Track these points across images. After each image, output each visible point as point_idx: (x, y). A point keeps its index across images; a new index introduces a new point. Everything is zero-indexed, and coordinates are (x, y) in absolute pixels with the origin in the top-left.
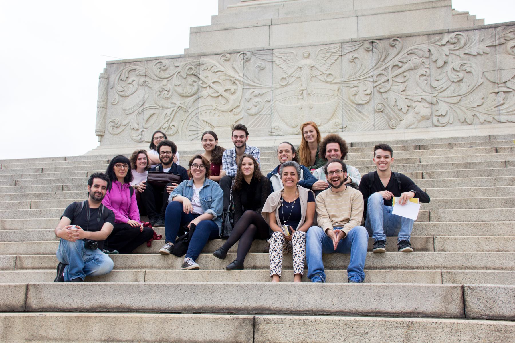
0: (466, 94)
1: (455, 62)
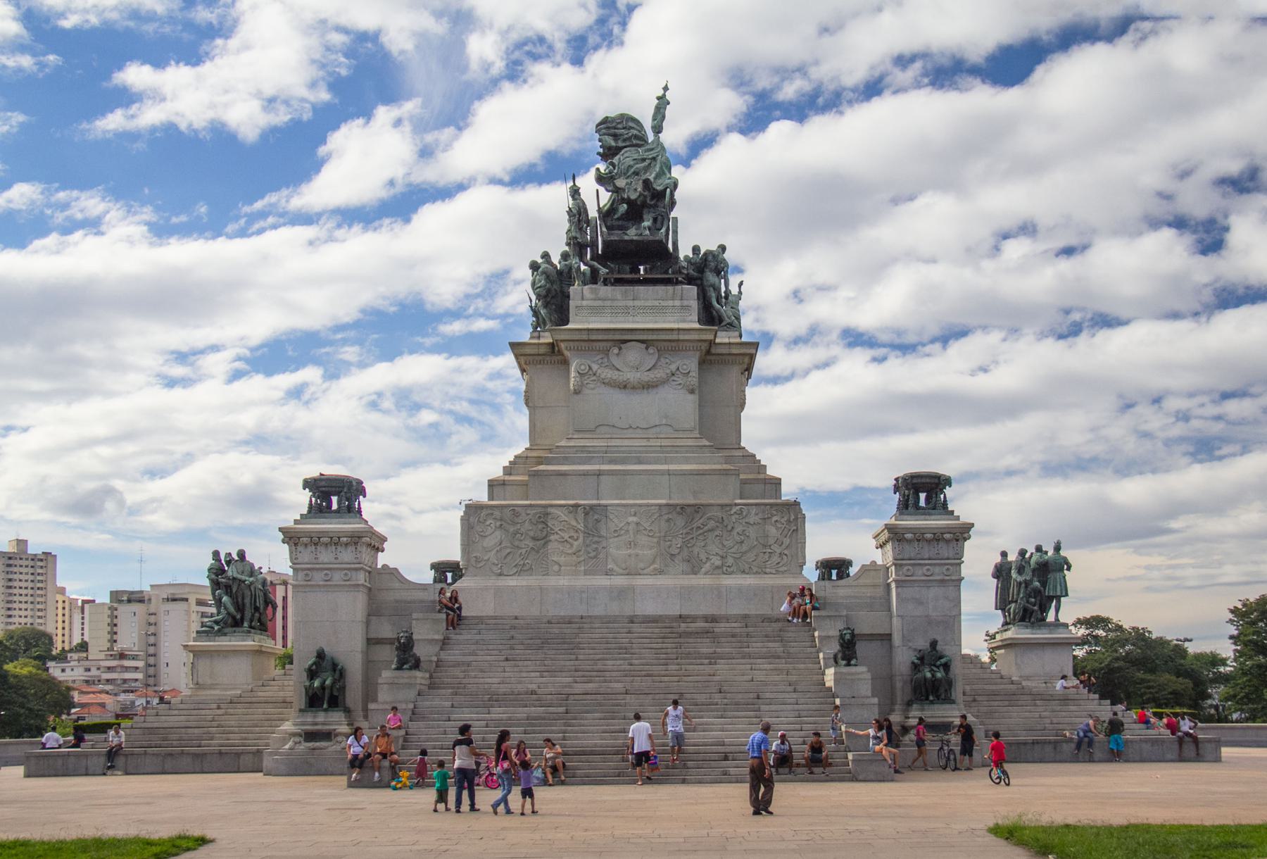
0: (745, 552)
1: (739, 529)
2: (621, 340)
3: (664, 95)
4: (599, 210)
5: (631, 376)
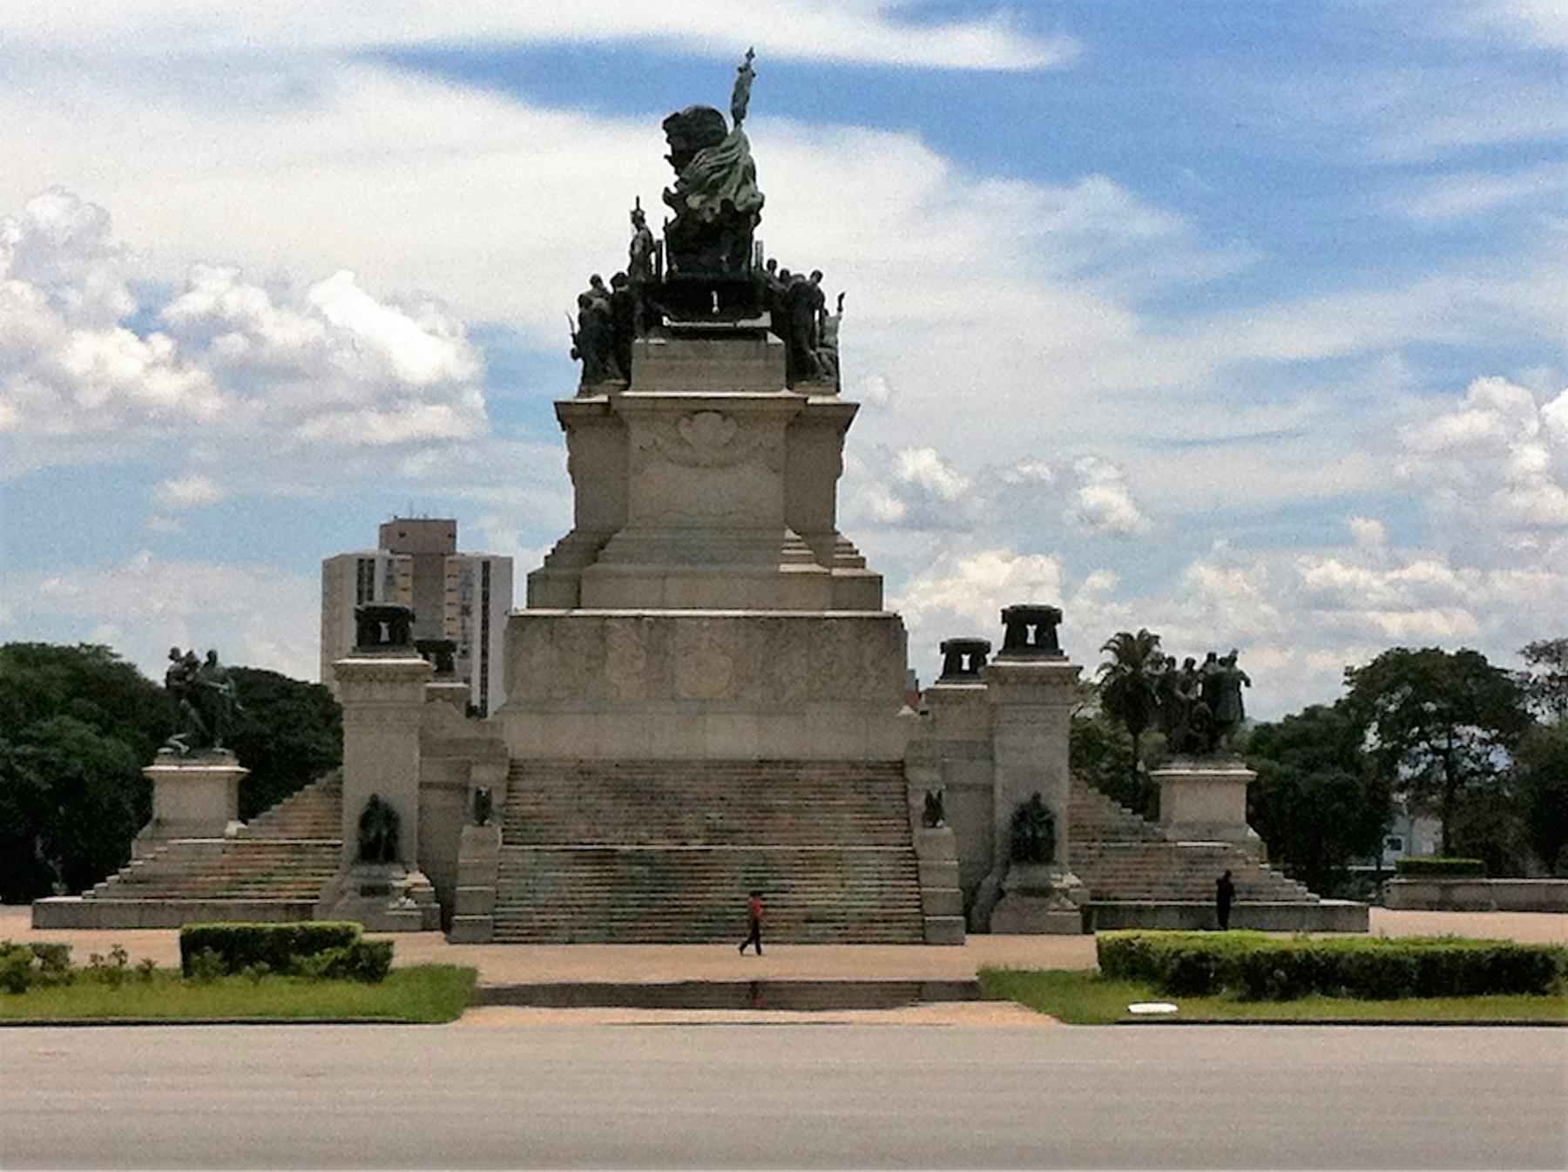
2: (694, 409)
3: (748, 66)
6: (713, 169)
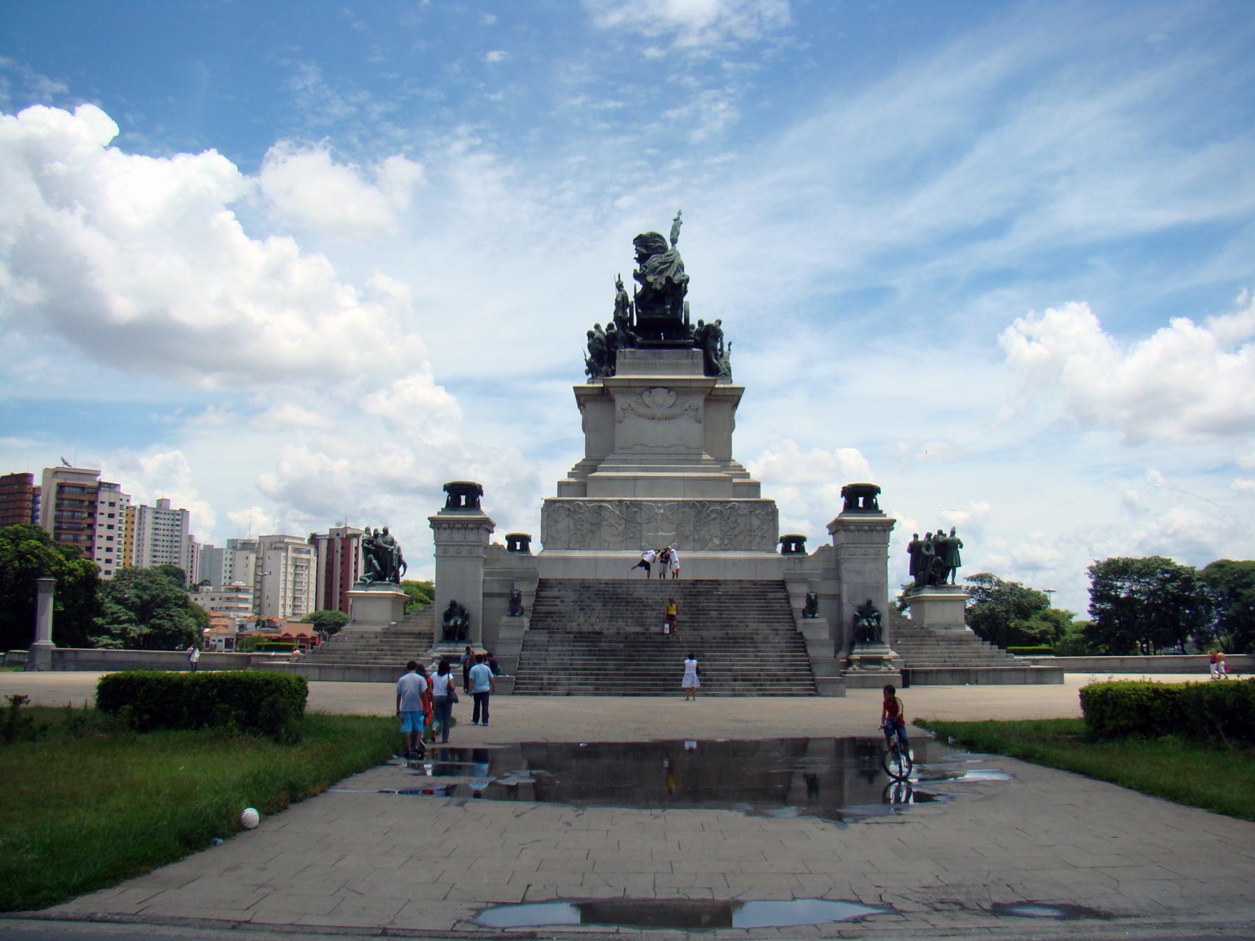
1: (733, 519)
2: (651, 386)
4: (636, 296)
5: (659, 412)
6: (661, 264)
